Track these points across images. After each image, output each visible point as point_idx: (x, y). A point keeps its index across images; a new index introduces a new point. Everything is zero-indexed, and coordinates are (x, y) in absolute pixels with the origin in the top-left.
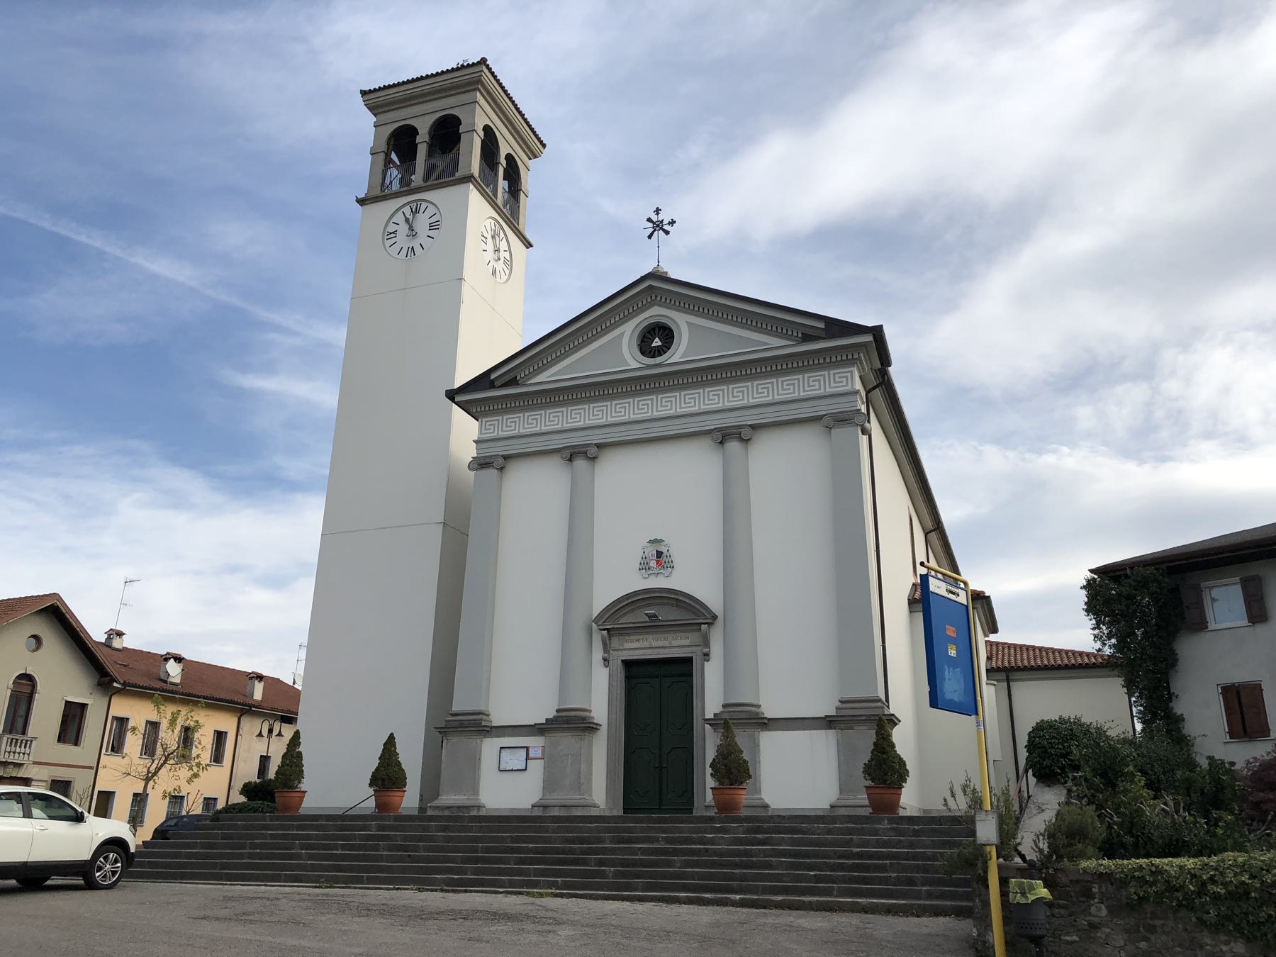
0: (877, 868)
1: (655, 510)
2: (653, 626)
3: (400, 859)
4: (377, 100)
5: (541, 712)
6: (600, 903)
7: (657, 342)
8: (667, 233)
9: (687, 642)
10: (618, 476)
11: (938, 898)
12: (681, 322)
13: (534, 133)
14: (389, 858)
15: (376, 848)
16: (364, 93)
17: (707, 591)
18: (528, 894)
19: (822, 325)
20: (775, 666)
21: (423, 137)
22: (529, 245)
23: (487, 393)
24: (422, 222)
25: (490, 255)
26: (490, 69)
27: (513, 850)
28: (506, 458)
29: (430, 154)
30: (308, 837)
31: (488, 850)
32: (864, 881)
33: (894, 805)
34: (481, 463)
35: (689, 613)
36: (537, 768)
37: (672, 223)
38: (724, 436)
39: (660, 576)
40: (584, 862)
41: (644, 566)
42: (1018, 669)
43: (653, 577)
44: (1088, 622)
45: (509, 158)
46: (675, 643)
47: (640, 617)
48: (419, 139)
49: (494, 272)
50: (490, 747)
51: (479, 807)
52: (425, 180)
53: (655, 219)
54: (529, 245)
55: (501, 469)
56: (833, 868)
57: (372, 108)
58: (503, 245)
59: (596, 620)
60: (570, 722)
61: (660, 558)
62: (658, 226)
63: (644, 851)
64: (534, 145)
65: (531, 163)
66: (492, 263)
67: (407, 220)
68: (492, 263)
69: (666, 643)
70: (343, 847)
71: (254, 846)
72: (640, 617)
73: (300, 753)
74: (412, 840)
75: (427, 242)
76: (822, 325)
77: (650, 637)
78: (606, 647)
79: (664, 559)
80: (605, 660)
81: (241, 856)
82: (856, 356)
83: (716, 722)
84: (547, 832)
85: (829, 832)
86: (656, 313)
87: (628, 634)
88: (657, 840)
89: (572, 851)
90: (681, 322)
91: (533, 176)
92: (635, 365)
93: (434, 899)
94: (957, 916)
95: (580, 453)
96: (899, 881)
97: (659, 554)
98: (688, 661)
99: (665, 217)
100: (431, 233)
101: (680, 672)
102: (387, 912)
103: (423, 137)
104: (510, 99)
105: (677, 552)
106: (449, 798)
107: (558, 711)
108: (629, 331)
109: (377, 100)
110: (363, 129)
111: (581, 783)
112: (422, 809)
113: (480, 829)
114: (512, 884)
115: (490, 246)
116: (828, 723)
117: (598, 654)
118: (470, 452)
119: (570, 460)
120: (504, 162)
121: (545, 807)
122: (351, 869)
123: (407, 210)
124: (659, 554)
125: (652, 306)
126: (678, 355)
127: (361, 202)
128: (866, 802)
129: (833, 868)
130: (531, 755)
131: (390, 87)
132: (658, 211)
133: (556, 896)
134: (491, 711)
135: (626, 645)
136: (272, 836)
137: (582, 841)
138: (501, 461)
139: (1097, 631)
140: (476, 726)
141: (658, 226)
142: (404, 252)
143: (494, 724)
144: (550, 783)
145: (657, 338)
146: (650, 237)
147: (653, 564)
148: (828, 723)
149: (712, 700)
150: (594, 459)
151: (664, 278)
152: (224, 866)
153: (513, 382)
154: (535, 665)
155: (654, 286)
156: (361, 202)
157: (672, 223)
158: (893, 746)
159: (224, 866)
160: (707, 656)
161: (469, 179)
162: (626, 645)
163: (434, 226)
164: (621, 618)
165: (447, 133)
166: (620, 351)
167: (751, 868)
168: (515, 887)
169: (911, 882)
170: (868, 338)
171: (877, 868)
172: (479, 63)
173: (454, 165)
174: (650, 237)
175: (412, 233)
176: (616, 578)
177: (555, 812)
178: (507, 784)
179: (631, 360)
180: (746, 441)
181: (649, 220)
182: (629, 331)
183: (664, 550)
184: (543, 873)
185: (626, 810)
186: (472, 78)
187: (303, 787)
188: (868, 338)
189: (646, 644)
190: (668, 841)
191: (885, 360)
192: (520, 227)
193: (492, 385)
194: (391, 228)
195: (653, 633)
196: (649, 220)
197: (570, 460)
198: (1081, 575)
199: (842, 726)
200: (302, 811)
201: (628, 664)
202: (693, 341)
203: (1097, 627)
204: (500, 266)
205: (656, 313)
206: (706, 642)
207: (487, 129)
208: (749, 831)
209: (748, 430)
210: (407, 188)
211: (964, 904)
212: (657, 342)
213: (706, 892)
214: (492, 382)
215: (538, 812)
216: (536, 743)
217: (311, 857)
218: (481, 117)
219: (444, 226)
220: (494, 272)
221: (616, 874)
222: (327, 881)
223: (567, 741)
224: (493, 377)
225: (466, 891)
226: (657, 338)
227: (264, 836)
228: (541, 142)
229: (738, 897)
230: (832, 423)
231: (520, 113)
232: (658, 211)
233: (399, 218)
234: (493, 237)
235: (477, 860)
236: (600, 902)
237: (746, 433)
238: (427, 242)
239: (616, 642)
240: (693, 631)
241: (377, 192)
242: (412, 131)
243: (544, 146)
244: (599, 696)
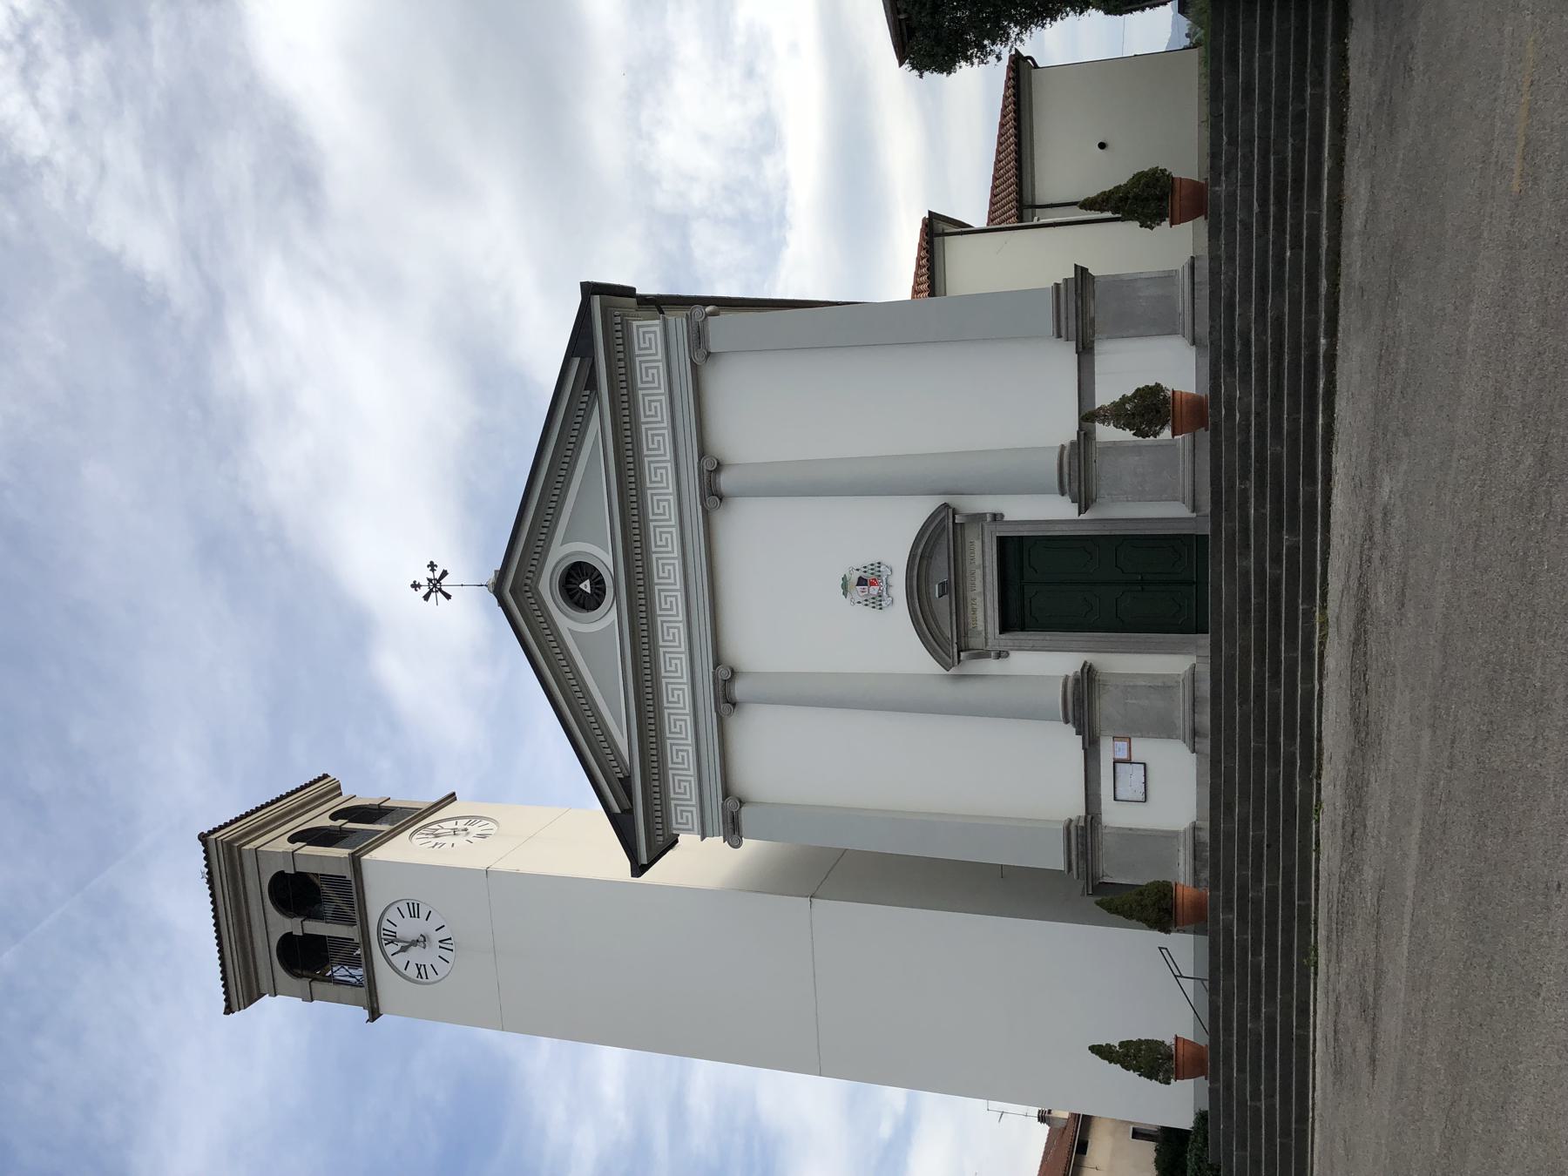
0: (1281, 172)
1: (805, 593)
2: (955, 589)
3: (1274, 860)
4: (241, 990)
5: (1070, 743)
6: (1335, 540)
7: (586, 586)
8: (445, 573)
9: (978, 544)
10: (757, 643)
11: (1322, 74)
12: (562, 552)
13: (307, 786)
14: (1273, 878)
15: (1257, 903)
16: (229, 1010)
17: (913, 515)
18: (1322, 644)
19: (576, 361)
20: (1008, 426)
21: (294, 926)
22: (452, 797)
23: (642, 833)
24: (407, 928)
25: (460, 840)
26: (215, 830)
27: (1260, 696)
28: (726, 794)
29: (318, 917)
30: (1242, 1014)
31: (1260, 732)
32: (1298, 180)
33: (1197, 190)
34: (733, 831)
35: (940, 539)
36: (1143, 748)
37: (432, 566)
38: (712, 494)
39: (891, 581)
40: (1276, 582)
41: (877, 602)
42: (1020, 192)
43: (892, 591)
44: (964, 71)
45: (334, 817)
46: (978, 561)
47: (943, 606)
48: (298, 932)
49: (483, 836)
50: (1114, 816)
51: (1195, 828)
52: (352, 923)
53: (425, 590)
54: (452, 797)
55: (742, 802)
56: (1280, 229)
57: (252, 996)
58: (451, 824)
59: (947, 667)
60: (1082, 704)
61: (867, 581)
62: (435, 586)
63: (1260, 504)
64: (323, 788)
65: (346, 792)
66: (470, 838)
67: (404, 949)
68: (470, 838)
69: (979, 573)
70: (1256, 953)
71: (1256, 1095)
72: (943, 606)
73: (1122, 1044)
74: (1246, 905)
75: (436, 920)
76: (576, 361)
77: (970, 595)
78: (982, 655)
79: (867, 576)
80: (999, 656)
81: (1271, 1109)
82: (618, 320)
83: (1085, 501)
84: (1233, 656)
85: (1231, 259)
86: (547, 587)
87: (966, 625)
88: (1245, 492)
89: (1260, 609)
90: (562, 552)
91: (360, 792)
92: (613, 614)
93: (1336, 657)
94: (1346, 36)
95: (725, 694)
96: (1299, 134)
97: (862, 582)
98: (1002, 542)
99: (423, 576)
100: (423, 914)
101: (1019, 553)
102: (1353, 836)
103: (294, 926)
104: (258, 809)
105: (858, 558)
106: (1182, 874)
107: (1067, 722)
108: (568, 623)
109: (241, 990)
110: (281, 1013)
111: (1163, 686)
112: (1197, 919)
113: (1230, 755)
114: (1308, 678)
115: (448, 840)
116: (1085, 351)
117: (991, 666)
118: (717, 842)
119: (734, 705)
120: (340, 822)
121: (1195, 733)
122: (1288, 931)
123: (391, 949)
124: (862, 582)
125: (535, 588)
126: (603, 556)
127: (374, 1014)
128: (1187, 437)
129: (1280, 229)
130: (1125, 756)
131: (224, 972)
132: (416, 586)
133: (1324, 608)
134: (1065, 818)
135: (981, 627)
136: (1241, 1070)
137: (1245, 599)
138: (730, 802)
139: (976, 61)
140: (1085, 834)
141: (435, 586)
142: (445, 954)
143: (1083, 813)
144: (1161, 729)
145: (581, 587)
146: (448, 597)
147: (874, 590)
148: (1085, 351)
149: (1052, 510)
150: (734, 673)
151: (501, 575)
152: (1286, 1133)
153: (626, 783)
154: (1002, 757)
155: (512, 589)
156: (374, 1014)
157: (432, 566)
158: (1118, 188)
159: (1286, 1133)
160: (997, 517)
161: (355, 861)
162: (981, 627)
163: (414, 911)
164: (946, 638)
165: (295, 891)
166: (594, 635)
167: (1281, 345)
168: (1311, 660)
169: (1300, 117)
170: (596, 300)
171: (1281, 172)
172: (205, 843)
173: (338, 882)
174: (448, 597)
175: (422, 941)
176: (891, 642)
177: (1205, 720)
178: (1164, 792)
179: (607, 620)
180: (719, 467)
181: (426, 597)
182: (568, 623)
183: (856, 575)
184: (1292, 638)
185: (1200, 629)
186: (224, 854)
187: (1170, 1041)
188: (596, 300)
189: (979, 600)
190: (1245, 477)
191: (628, 292)
192: (425, 807)
193: (629, 812)
194: (412, 972)
195: (963, 561)
196: (426, 597)
197: (734, 705)
198: (906, 73)
199: (1090, 331)
200: (1204, 1041)
201: (1005, 627)
202: (587, 538)
203: (968, 59)
204: (475, 830)
205: (547, 587)
206: (978, 518)
207: (292, 840)
208: (1230, 368)
209: (704, 461)
210: (357, 954)
211: (1330, 19)
212: (586, 586)
213: (1316, 387)
214: (624, 811)
215: (1205, 745)
216: (1109, 750)
217: (1271, 997)
218: (278, 844)
219: (414, 896)
220: (483, 836)
221: (1293, 530)
222: (1307, 955)
223: (1106, 707)
224: (617, 810)
225: (1320, 740)
226: (581, 587)
227: (1242, 1082)
228: (320, 779)
229: (1323, 341)
230: (703, 351)
231: (278, 800)
232: (416, 586)
233: (399, 961)
234: (437, 836)
235: (1274, 743)
236: (1337, 426)
237: (708, 465)
238: (436, 920)
239: (976, 642)
240: (963, 536)
241: (363, 992)
242: (287, 941)
243: (325, 776)
244: (1047, 664)
